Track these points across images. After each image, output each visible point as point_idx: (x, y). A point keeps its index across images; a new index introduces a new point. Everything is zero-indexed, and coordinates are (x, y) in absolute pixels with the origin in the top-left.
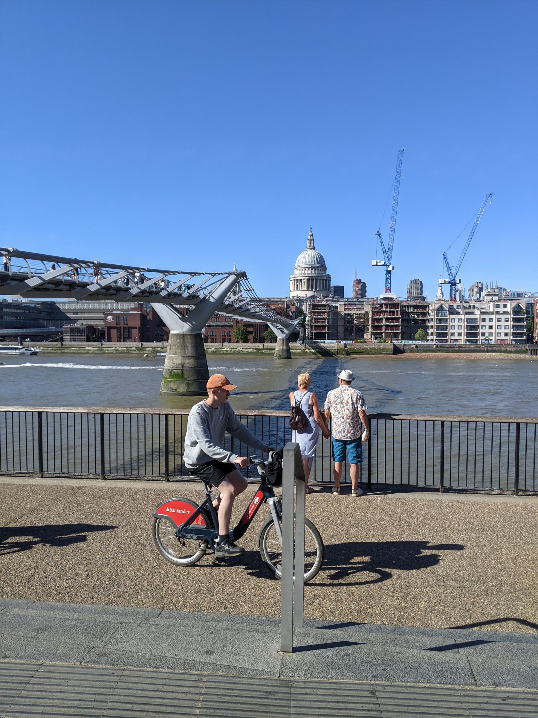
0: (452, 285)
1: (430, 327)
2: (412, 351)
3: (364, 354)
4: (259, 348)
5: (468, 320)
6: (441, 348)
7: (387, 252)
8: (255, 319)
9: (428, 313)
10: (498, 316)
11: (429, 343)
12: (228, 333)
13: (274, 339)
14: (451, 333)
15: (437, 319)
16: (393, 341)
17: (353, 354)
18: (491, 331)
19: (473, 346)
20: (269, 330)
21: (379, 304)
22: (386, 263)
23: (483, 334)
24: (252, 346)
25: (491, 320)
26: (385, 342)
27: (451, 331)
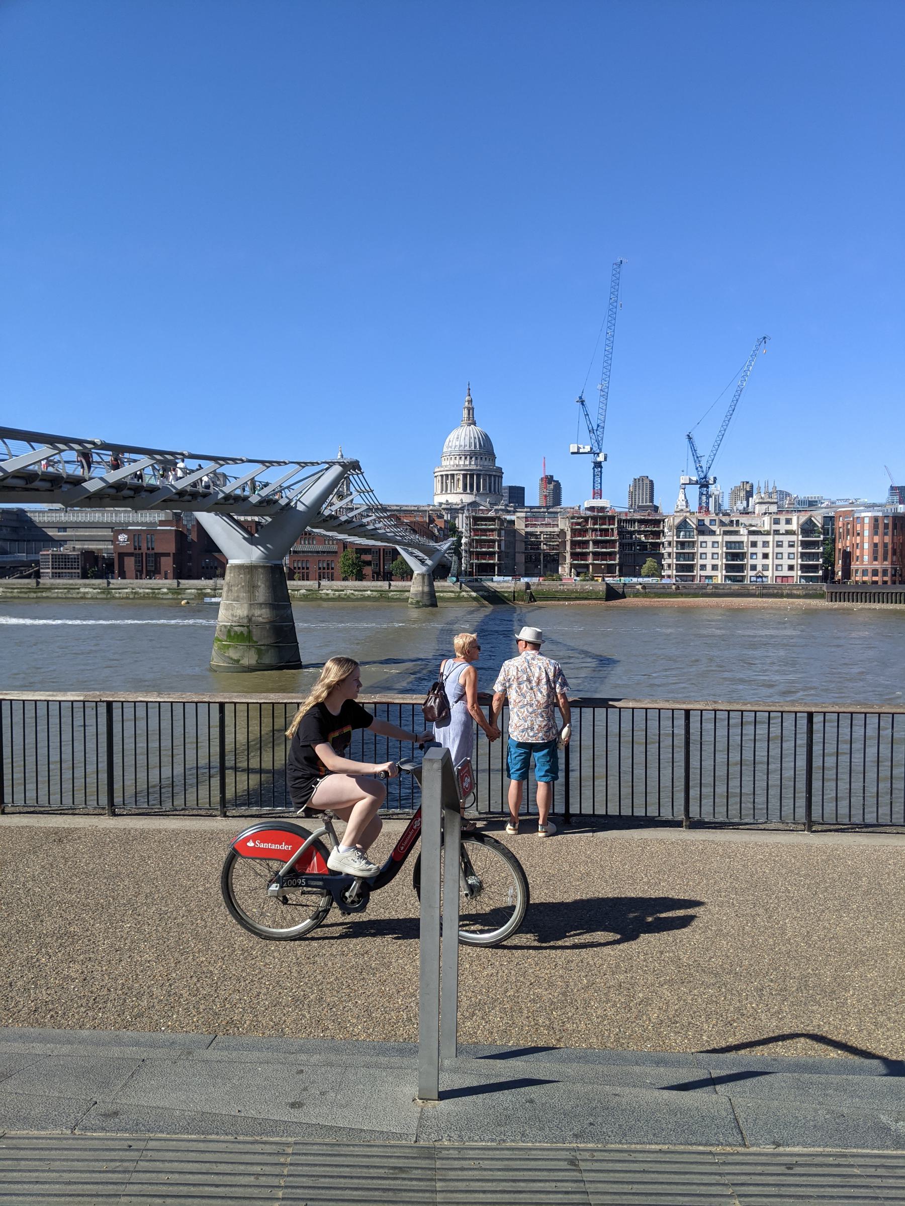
0: (702, 486)
1: (666, 556)
2: (637, 595)
4: (383, 589)
5: (729, 544)
8: (376, 540)
9: (663, 532)
10: (777, 538)
11: (664, 581)
12: (328, 564)
13: (407, 574)
14: (701, 566)
16: (607, 579)
17: (542, 599)
18: (766, 562)
19: (737, 587)
20: (399, 559)
21: (582, 518)
22: (594, 449)
23: (754, 568)
24: (371, 586)
25: (766, 544)
26: (592, 580)
27: (701, 562)
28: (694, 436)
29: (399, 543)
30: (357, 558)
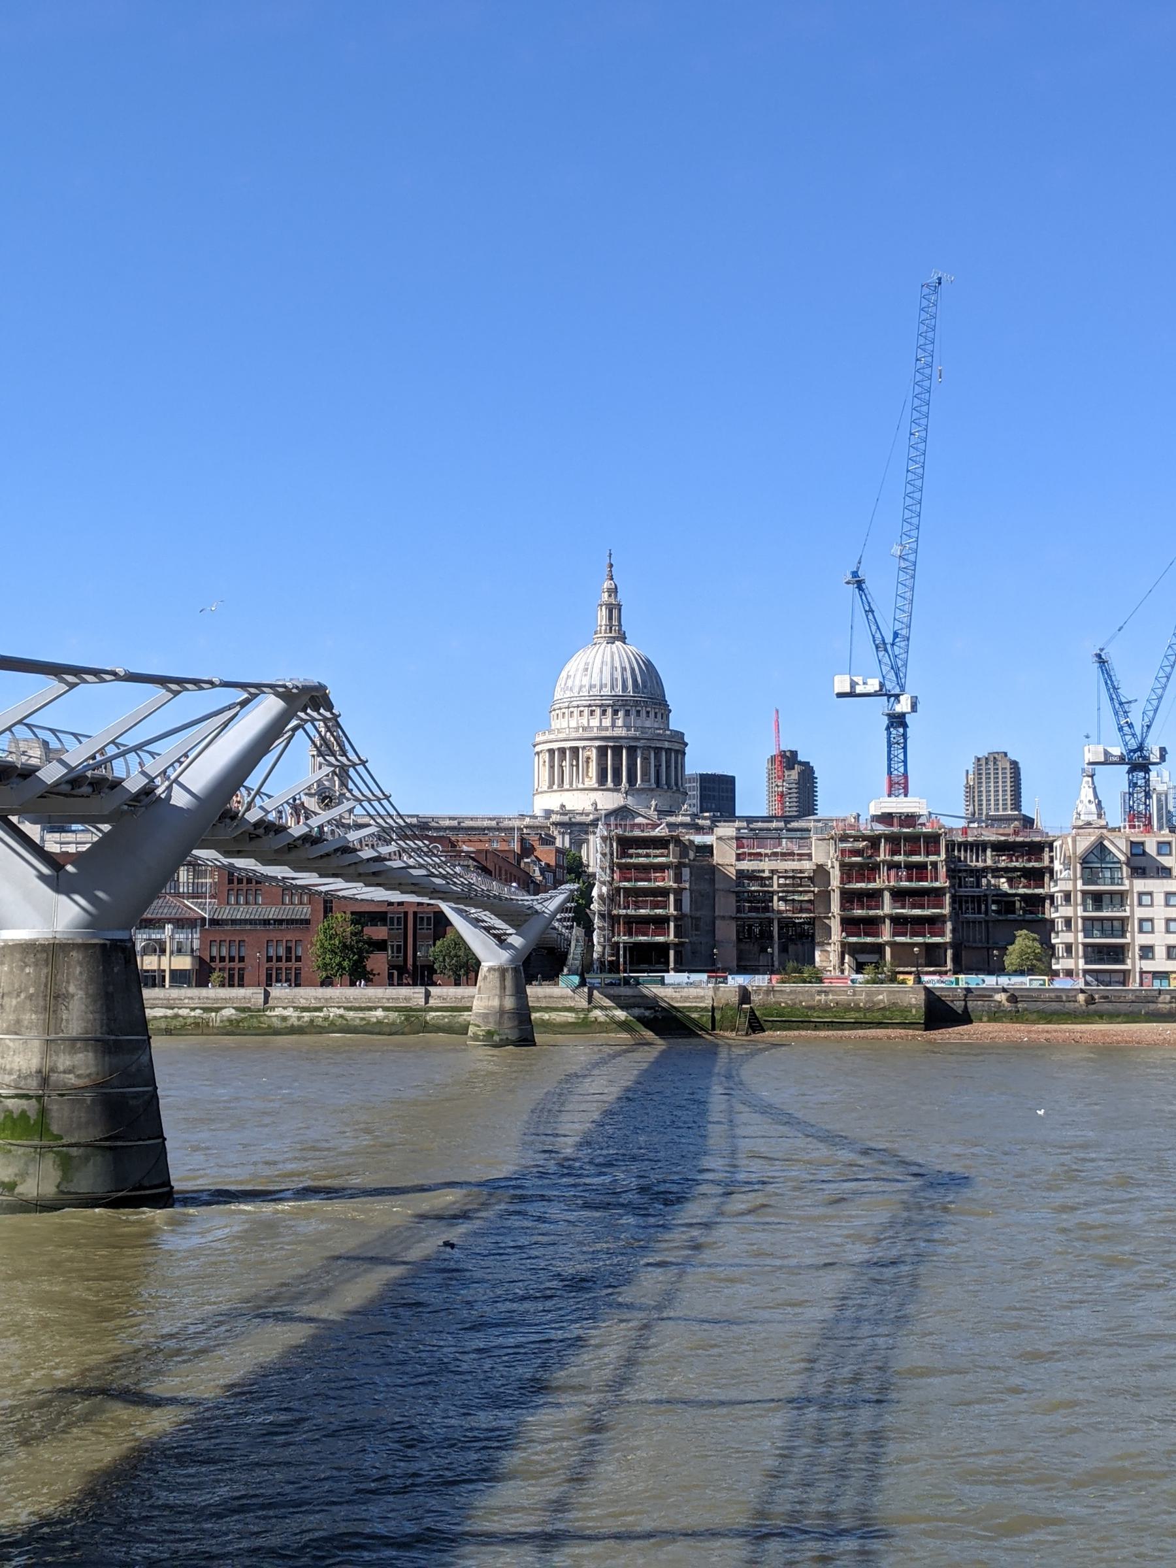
1: (1060, 925)
2: (996, 1015)
3: (817, 1026)
6: (1107, 1006)
7: (890, 647)
9: (1051, 871)
11: (1061, 983)
12: (289, 949)
13: (466, 969)
14: (1142, 948)
15: (1084, 893)
16: (925, 978)
17: (775, 1026)
20: (450, 935)
21: (865, 838)
24: (380, 999)
26: (893, 980)
27: (1142, 939)
28: (1111, 654)
29: (445, 895)
30: (353, 934)
